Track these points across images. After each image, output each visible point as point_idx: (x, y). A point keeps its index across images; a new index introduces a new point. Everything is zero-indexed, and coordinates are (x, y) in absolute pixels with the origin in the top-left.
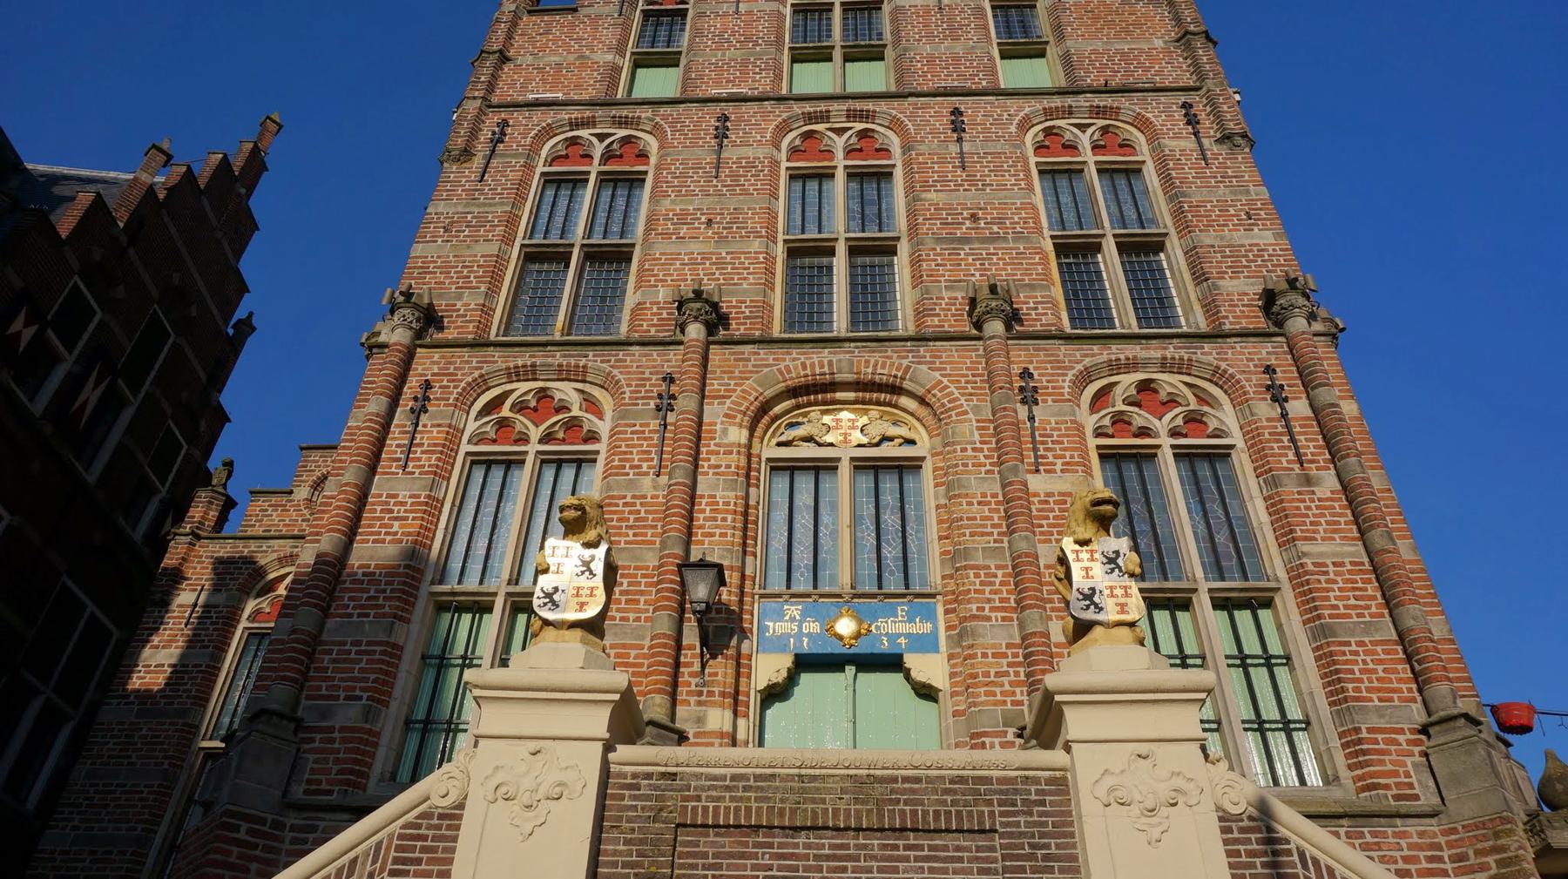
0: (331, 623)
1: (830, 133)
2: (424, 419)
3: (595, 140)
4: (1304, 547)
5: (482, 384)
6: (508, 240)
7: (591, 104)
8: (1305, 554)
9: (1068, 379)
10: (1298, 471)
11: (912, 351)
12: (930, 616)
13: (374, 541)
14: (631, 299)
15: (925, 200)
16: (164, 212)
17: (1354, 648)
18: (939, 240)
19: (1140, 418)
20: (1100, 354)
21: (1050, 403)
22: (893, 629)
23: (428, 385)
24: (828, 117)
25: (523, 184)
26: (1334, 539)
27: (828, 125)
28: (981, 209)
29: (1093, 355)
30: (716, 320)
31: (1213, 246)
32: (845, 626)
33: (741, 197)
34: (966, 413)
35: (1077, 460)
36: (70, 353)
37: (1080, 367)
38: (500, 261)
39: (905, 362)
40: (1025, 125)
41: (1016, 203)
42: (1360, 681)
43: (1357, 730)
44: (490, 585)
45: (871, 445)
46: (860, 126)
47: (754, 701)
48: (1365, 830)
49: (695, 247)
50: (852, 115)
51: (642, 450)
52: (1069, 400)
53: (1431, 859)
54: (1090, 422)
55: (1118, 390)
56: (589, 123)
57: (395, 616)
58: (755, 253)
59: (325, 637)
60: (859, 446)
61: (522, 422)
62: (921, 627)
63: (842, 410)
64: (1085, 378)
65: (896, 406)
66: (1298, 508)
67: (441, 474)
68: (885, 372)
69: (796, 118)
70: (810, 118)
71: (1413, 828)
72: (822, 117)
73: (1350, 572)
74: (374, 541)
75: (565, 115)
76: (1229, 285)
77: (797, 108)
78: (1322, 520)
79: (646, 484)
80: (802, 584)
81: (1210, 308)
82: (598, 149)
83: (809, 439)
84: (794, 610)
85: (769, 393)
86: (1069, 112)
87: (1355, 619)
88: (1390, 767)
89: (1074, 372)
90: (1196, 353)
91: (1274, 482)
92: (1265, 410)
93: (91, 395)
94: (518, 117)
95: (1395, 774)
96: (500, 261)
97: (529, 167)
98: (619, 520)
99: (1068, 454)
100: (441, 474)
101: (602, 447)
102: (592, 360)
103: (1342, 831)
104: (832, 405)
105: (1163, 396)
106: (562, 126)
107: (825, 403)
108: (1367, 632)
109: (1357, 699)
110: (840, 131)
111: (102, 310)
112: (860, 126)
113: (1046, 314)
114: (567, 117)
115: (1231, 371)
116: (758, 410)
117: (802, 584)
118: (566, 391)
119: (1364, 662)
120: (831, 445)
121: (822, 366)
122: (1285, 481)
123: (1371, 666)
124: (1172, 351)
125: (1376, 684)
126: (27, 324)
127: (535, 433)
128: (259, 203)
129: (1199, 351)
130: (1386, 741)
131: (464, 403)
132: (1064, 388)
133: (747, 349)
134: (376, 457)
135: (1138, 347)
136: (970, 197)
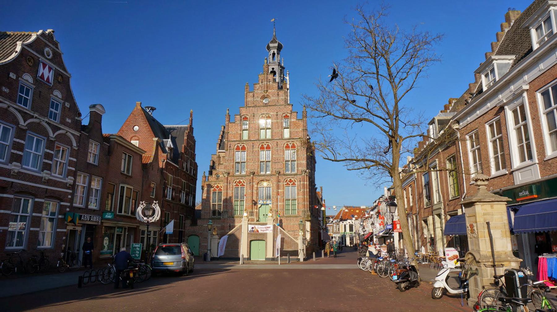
5: (234, 180)
12: (271, 201)
19: (289, 183)
22: (268, 202)
32: (265, 202)
40: (284, 145)
46: (267, 144)
47: (258, 208)
49: (252, 164)
50: (266, 143)
54: (285, 183)
55: (288, 180)
56: (239, 144)
62: (270, 202)
64: (285, 179)
70: (262, 143)
75: (237, 143)
76: (299, 168)
77: (261, 142)
79: (249, 191)
80: (262, 199)
82: (241, 148)
84: (261, 201)
86: (289, 142)
91: (298, 190)
92: (299, 183)
94: (232, 143)
96: (233, 165)
97: (234, 151)
100: (233, 190)
101: (245, 186)
102: (243, 178)
112: (267, 144)
117: (262, 199)
118: (241, 180)
124: (293, 176)
127: (240, 185)
128: (193, 127)
131: (233, 183)
136: (277, 156)
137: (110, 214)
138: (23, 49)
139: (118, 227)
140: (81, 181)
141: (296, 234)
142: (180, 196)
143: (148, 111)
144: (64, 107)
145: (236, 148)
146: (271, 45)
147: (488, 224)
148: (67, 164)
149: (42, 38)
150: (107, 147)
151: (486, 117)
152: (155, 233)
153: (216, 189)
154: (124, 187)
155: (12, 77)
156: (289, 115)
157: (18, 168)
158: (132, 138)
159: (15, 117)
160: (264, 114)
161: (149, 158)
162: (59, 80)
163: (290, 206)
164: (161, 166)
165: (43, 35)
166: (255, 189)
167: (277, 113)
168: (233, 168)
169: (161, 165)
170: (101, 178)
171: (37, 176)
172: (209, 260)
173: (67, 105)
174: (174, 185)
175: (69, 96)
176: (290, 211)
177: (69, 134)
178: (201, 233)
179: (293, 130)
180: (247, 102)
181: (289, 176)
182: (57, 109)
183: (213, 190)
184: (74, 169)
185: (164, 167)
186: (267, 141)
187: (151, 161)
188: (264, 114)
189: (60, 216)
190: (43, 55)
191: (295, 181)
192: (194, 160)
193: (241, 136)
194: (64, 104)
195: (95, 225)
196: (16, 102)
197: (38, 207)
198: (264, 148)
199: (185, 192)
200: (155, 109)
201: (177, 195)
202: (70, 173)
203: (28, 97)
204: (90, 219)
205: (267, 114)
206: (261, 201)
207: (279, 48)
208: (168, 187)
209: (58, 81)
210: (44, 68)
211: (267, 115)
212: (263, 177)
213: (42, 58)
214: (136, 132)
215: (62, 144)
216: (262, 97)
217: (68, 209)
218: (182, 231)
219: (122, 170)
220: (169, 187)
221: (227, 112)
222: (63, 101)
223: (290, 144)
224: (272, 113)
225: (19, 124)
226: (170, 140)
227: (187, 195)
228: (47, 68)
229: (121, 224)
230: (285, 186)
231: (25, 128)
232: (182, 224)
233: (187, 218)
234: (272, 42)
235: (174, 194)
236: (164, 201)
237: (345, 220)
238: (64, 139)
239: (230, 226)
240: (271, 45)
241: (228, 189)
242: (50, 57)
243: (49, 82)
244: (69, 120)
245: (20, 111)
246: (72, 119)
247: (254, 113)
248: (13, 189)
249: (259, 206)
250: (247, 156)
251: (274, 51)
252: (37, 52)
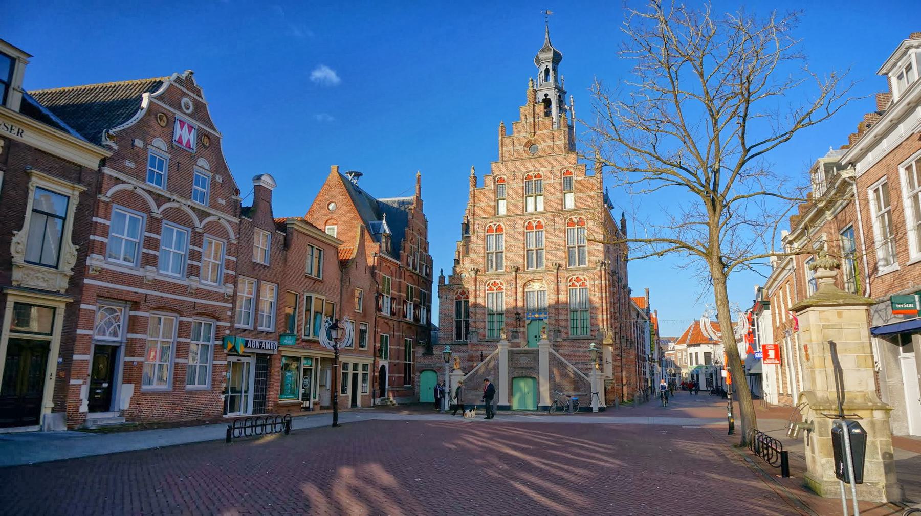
5: (486, 281)
6: (484, 253)
12: (546, 314)
14: (504, 264)
19: (576, 283)
20: (571, 273)
22: (542, 316)
25: (484, 239)
30: (517, 270)
32: (536, 315)
38: (484, 257)
46: (538, 220)
47: (526, 326)
49: (512, 253)
51: (509, 292)
55: (573, 279)
61: (493, 287)
62: (546, 316)
64: (569, 277)
67: (484, 297)
70: (529, 219)
75: (489, 220)
77: (527, 217)
81: (589, 263)
84: (530, 314)
94: (480, 221)
96: (484, 257)
97: (484, 234)
101: (504, 291)
112: (538, 220)
118: (498, 281)
127: (495, 289)
131: (485, 285)
134: (476, 295)
136: (554, 240)
137: (290, 338)
138: (151, 104)
139: (306, 358)
140: (246, 289)
142: (405, 309)
143: (350, 178)
144: (214, 183)
145: (487, 230)
146: (542, 56)
147: (833, 345)
148: (223, 266)
149: (177, 85)
150: (282, 238)
151: (899, 155)
152: (365, 366)
153: (461, 296)
154: (311, 297)
155: (138, 145)
156: (572, 171)
157: (153, 275)
158: (327, 221)
159: (145, 202)
160: (530, 171)
161: (350, 252)
162: (205, 144)
163: (578, 322)
164: (370, 263)
165: (178, 80)
166: (520, 294)
167: (552, 167)
168: (484, 263)
169: (371, 261)
170: (276, 285)
171: (179, 285)
172: (447, 408)
173: (219, 179)
174: (393, 292)
175: (220, 166)
176: (579, 330)
177: (222, 221)
178: (440, 367)
179: (579, 195)
180: (502, 154)
181: (576, 272)
182: (203, 187)
183: (456, 299)
184: (234, 273)
185: (375, 265)
186: (537, 216)
187: (353, 256)
188: (530, 171)
189: (217, 342)
190: (179, 108)
191: (585, 279)
192: (426, 250)
193: (495, 209)
194: (214, 177)
195: (270, 355)
196: (144, 180)
197: (183, 329)
198: (532, 228)
199: (413, 303)
200: (361, 175)
201: (399, 307)
202: (228, 279)
203: (162, 171)
204: (261, 346)
205: (535, 171)
206: (530, 314)
207: (557, 59)
208: (383, 295)
209: (203, 144)
210: (182, 127)
211: (537, 173)
212: (532, 275)
213: (179, 115)
214: (332, 212)
215: (215, 238)
216: (526, 144)
217: (228, 332)
218: (410, 364)
219: (308, 270)
220: (386, 295)
221: (472, 171)
222: (211, 174)
223: (576, 218)
224: (544, 169)
225: (151, 212)
226: (384, 222)
227: (416, 306)
228: (186, 126)
229: (308, 353)
230: (569, 288)
231: (159, 217)
232: (410, 353)
233: (417, 343)
234: (543, 51)
235: (394, 306)
236: (377, 319)
237: (699, 345)
238: (216, 229)
239: (482, 355)
240: (542, 56)
241: (478, 296)
242: (190, 111)
243: (190, 148)
244: (222, 202)
245: (150, 193)
246: (225, 199)
247: (514, 171)
248: (147, 304)
249: (528, 322)
250: (506, 241)
251: (547, 66)
252: (171, 105)
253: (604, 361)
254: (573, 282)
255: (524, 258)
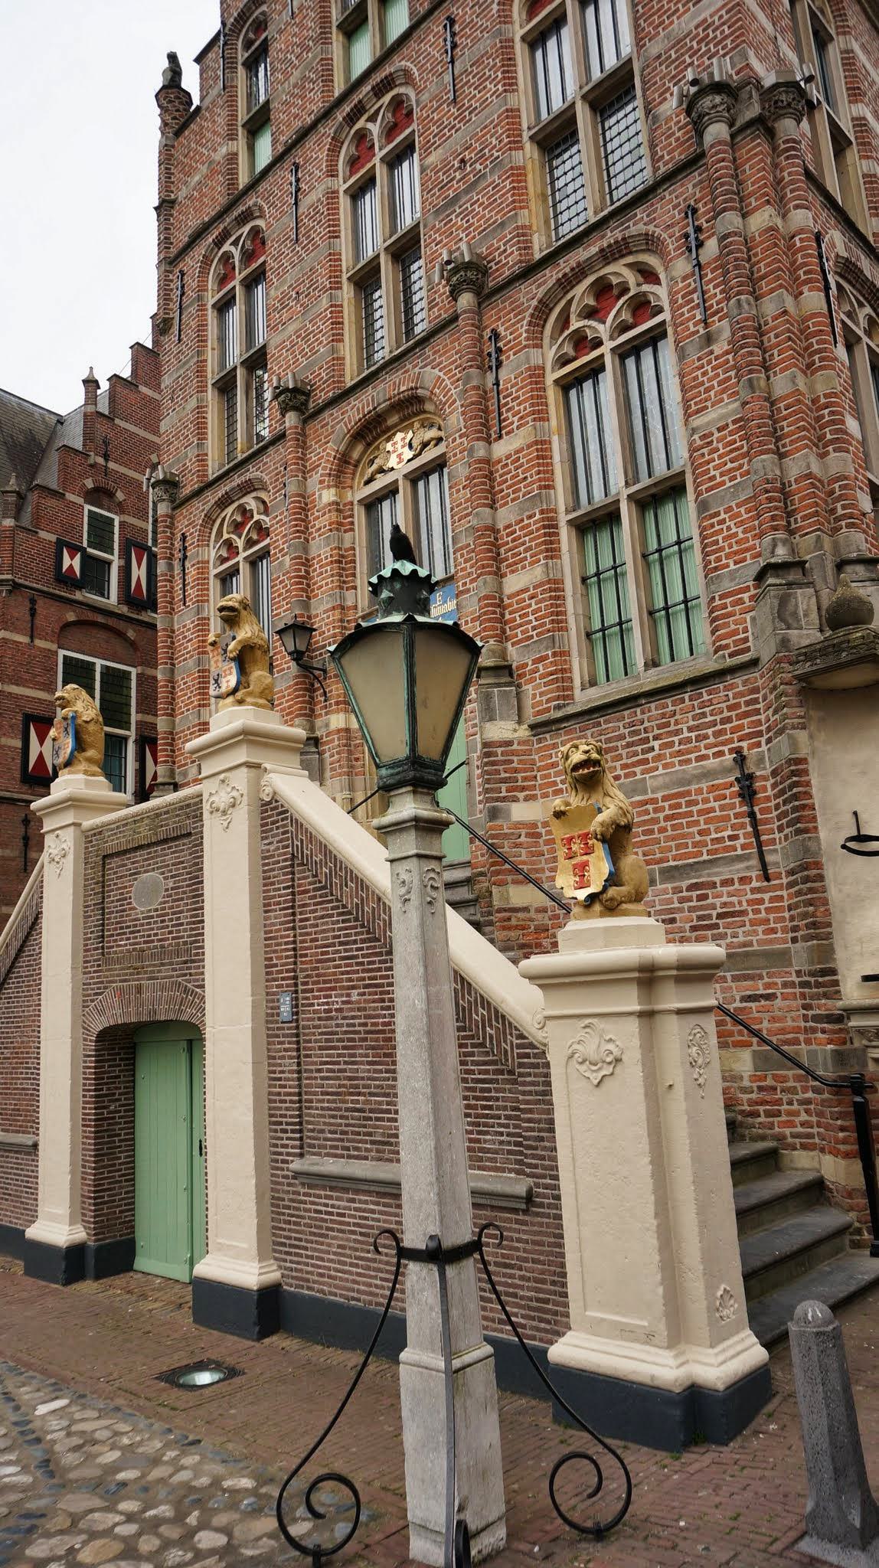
0: (177, 719)
1: (370, 125)
2: (187, 564)
3: (233, 249)
4: (697, 421)
7: (220, 216)
8: (694, 431)
9: (525, 322)
10: (702, 332)
11: (421, 355)
13: (184, 660)
15: (428, 167)
16: (117, 421)
17: (723, 516)
18: (437, 212)
20: (551, 276)
21: (512, 357)
23: (184, 538)
24: (363, 107)
25: (202, 327)
26: (722, 400)
27: (365, 117)
28: (467, 148)
29: (545, 282)
31: (659, 57)
33: (312, 254)
34: (454, 401)
35: (529, 410)
36: (112, 554)
37: (535, 302)
39: (417, 370)
41: (493, 120)
42: (722, 549)
43: (713, 598)
44: (676, 468)
45: (415, 457)
46: (387, 98)
48: (703, 690)
49: (292, 328)
50: (379, 91)
52: (525, 347)
53: (747, 703)
54: (551, 354)
57: (199, 706)
58: (326, 310)
59: (177, 730)
60: (409, 461)
63: (394, 434)
65: (425, 412)
66: (696, 378)
68: (405, 388)
69: (340, 128)
70: (352, 119)
71: (738, 681)
72: (380, 90)
73: (731, 433)
74: (184, 660)
78: (715, 383)
83: (381, 470)
85: (342, 448)
87: (728, 484)
88: (733, 627)
89: (531, 311)
90: (628, 227)
93: (139, 573)
95: (735, 632)
97: (202, 308)
98: (279, 596)
99: (522, 407)
103: (686, 696)
104: (388, 433)
105: (615, 292)
106: (212, 249)
107: (384, 432)
108: (734, 496)
109: (716, 569)
110: (372, 119)
111: (116, 513)
112: (387, 98)
113: (512, 253)
114: (211, 240)
115: (658, 230)
116: (338, 465)
119: (729, 528)
120: (392, 469)
121: (368, 406)
122: (689, 350)
123: (734, 530)
124: (611, 236)
125: (735, 548)
126: (72, 558)
129: (631, 223)
130: (735, 604)
131: (203, 541)
132: (520, 335)
133: (326, 414)
135: (581, 249)
141: (719, 899)
230: (551, 377)
253: (831, 834)
254: (575, 324)
255: (338, 323)
